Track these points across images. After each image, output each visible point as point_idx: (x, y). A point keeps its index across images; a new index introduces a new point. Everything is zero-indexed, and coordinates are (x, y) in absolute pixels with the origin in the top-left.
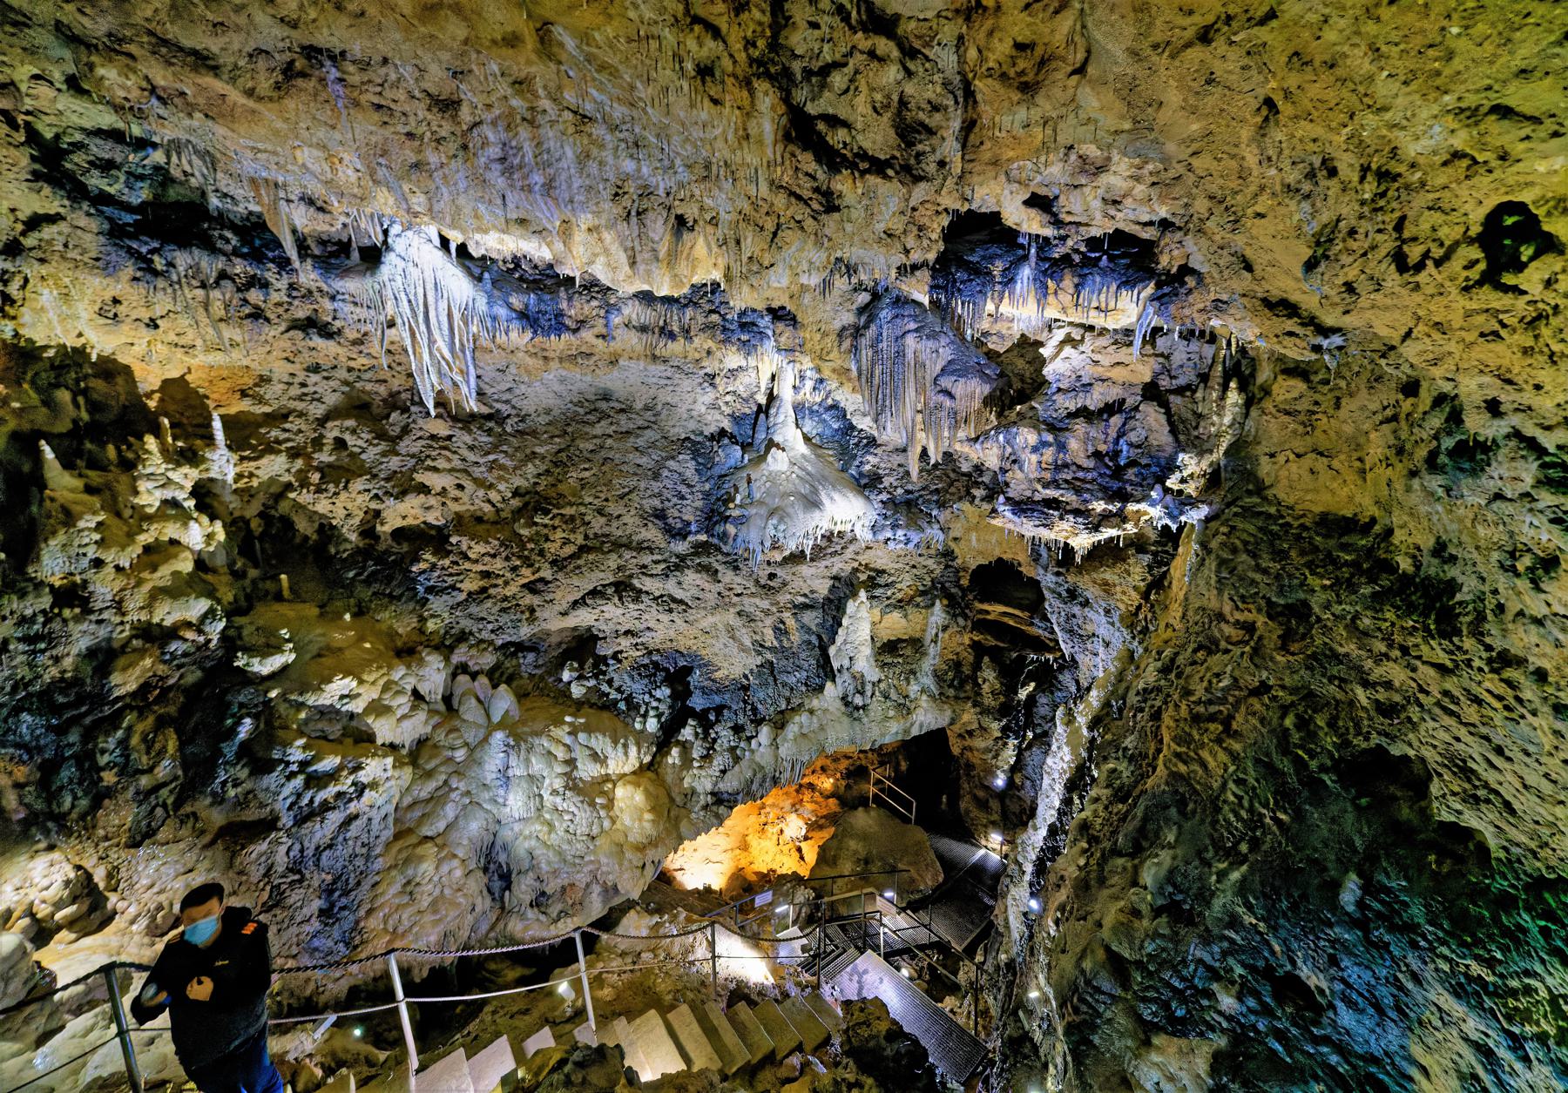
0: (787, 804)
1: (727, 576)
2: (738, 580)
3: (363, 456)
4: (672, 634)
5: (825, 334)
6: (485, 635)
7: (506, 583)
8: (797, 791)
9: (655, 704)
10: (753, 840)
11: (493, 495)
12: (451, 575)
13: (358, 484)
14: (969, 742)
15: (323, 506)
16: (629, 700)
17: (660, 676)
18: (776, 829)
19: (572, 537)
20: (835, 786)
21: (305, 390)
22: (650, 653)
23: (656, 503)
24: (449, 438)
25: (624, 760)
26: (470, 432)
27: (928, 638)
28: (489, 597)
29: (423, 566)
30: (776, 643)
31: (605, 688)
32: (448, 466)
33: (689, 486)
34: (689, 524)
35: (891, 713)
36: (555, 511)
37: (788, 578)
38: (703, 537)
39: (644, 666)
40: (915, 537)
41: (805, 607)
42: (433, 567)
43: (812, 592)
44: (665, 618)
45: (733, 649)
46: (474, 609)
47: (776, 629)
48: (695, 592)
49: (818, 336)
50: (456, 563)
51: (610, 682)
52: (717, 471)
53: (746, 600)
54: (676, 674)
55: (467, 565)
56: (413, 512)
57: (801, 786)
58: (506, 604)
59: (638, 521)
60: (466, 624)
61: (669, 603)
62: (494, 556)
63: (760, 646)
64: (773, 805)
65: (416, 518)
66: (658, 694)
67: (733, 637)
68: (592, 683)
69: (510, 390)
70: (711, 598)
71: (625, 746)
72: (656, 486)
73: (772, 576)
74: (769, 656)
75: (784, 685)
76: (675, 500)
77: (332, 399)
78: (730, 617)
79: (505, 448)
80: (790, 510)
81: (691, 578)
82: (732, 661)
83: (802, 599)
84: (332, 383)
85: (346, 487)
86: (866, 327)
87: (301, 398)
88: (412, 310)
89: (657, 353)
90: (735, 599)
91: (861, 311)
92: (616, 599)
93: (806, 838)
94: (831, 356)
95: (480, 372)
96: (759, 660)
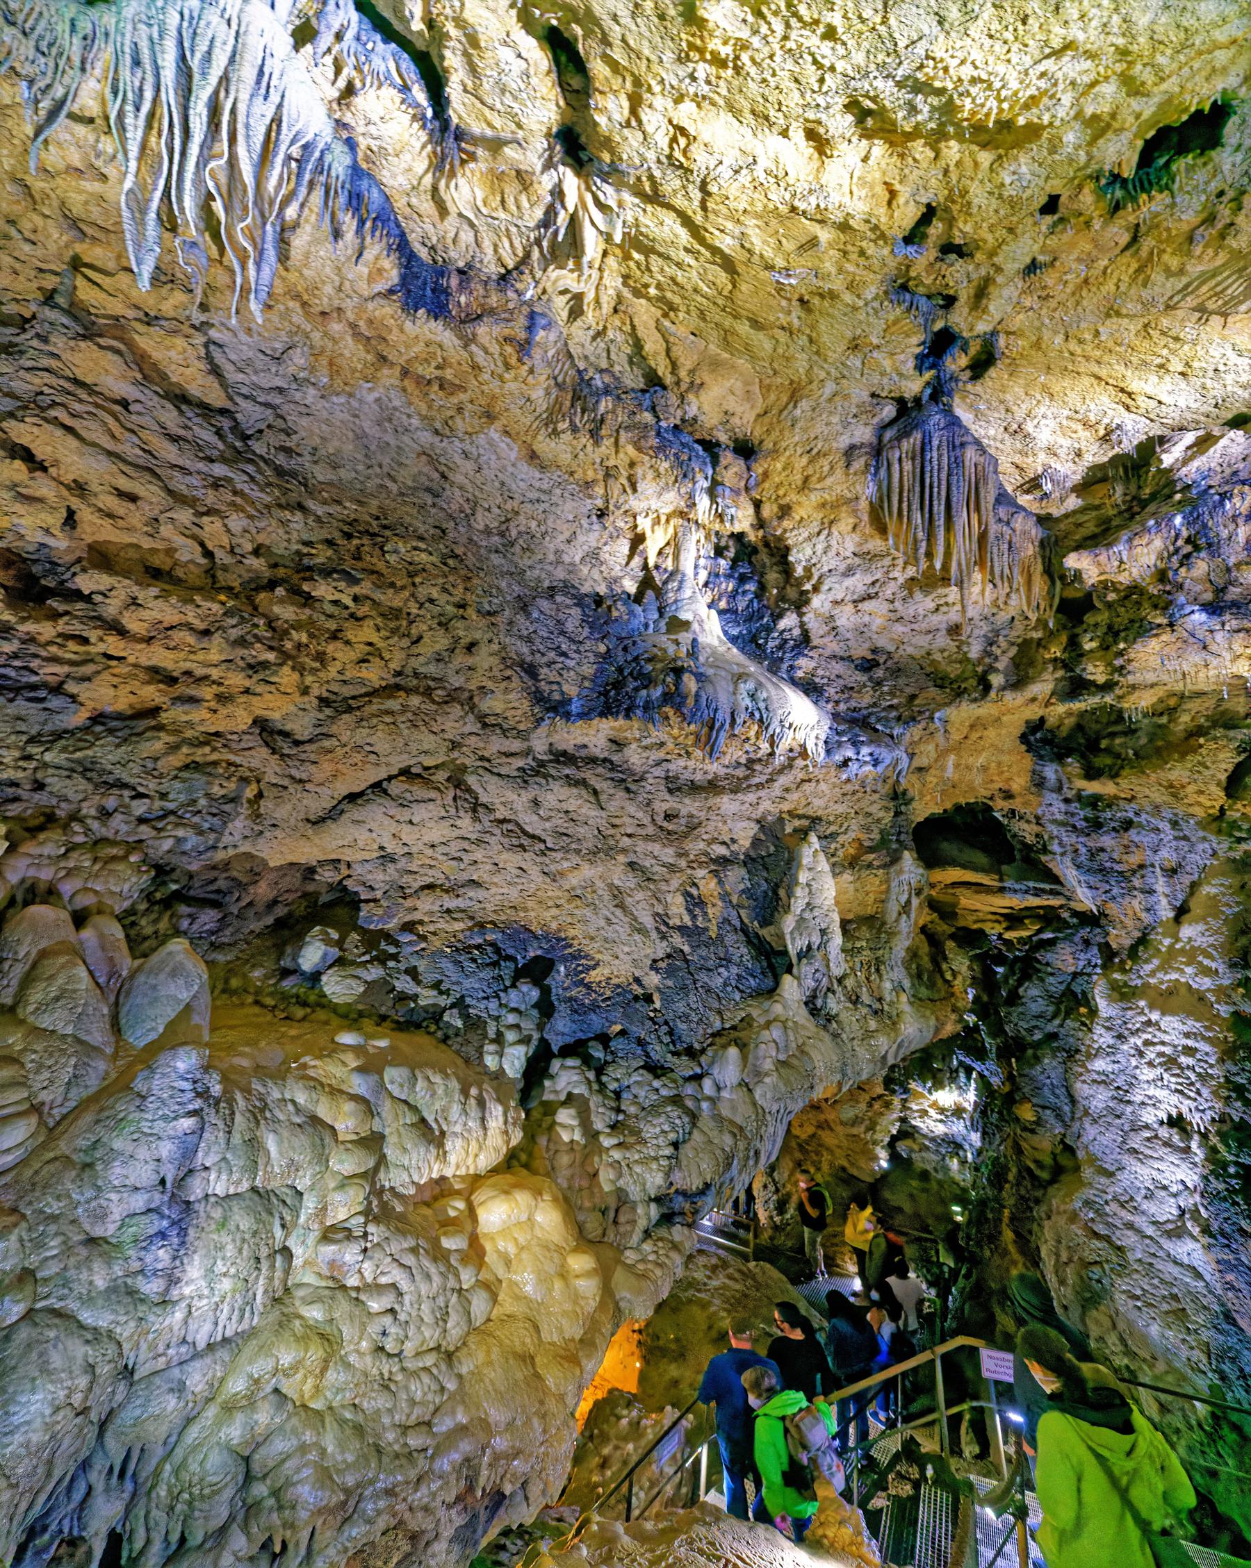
6: (119, 826)
9: (511, 1019)
11: (212, 529)
16: (460, 1004)
17: (507, 970)
22: (481, 926)
25: (478, 1140)
27: (892, 915)
28: (160, 728)
30: (687, 920)
31: (404, 984)
39: (478, 947)
41: (724, 862)
44: (511, 860)
45: (622, 928)
46: (106, 753)
48: (559, 822)
51: (413, 973)
53: (641, 846)
54: (533, 963)
60: (68, 790)
66: (513, 998)
68: (375, 973)
71: (481, 1103)
82: (621, 955)
90: (626, 841)
96: (661, 949)
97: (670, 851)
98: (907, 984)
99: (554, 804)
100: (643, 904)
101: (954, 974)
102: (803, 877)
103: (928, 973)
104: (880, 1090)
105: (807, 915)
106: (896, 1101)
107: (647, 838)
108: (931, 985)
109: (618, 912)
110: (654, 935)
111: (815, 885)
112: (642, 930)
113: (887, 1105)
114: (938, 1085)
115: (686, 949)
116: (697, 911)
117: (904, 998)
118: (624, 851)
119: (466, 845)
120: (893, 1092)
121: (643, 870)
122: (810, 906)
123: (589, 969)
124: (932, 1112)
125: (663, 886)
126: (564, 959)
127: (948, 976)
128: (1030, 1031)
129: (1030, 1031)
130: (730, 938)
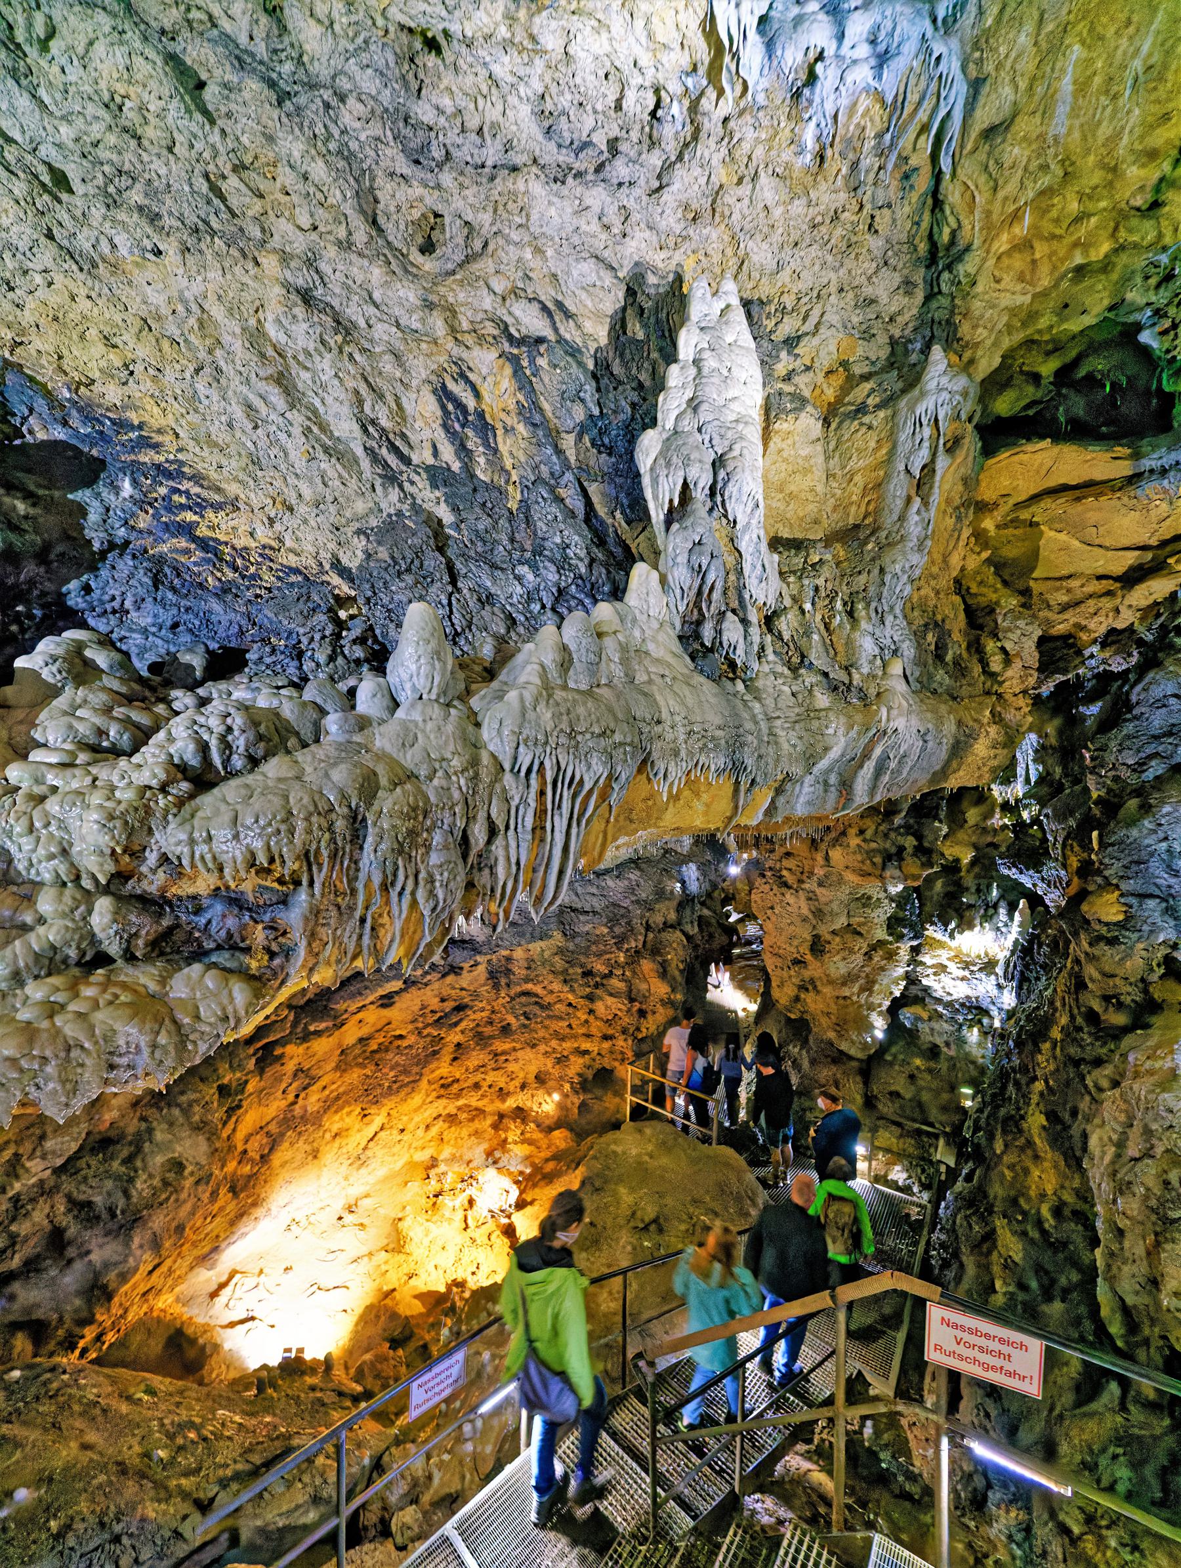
0: (478, 1153)
8: (495, 1127)
10: (416, 1229)
14: (814, 969)
18: (462, 1199)
20: (561, 1106)
30: (448, 454)
35: (822, 700)
57: (501, 1116)
64: (453, 1159)
67: (282, 380)
75: (487, 600)
93: (520, 1205)
97: (408, 293)
98: (908, 650)
100: (336, 391)
101: (1008, 659)
102: (688, 342)
103: (956, 646)
104: (881, 934)
105: (687, 425)
106: (904, 949)
108: (959, 669)
111: (710, 362)
112: (336, 452)
113: (891, 956)
114: (965, 924)
115: (444, 513)
116: (473, 442)
117: (896, 668)
120: (900, 937)
121: (343, 326)
122: (694, 405)
123: (199, 506)
124: (952, 966)
126: (135, 470)
127: (996, 665)
128: (1140, 767)
129: (1140, 767)
130: (545, 513)
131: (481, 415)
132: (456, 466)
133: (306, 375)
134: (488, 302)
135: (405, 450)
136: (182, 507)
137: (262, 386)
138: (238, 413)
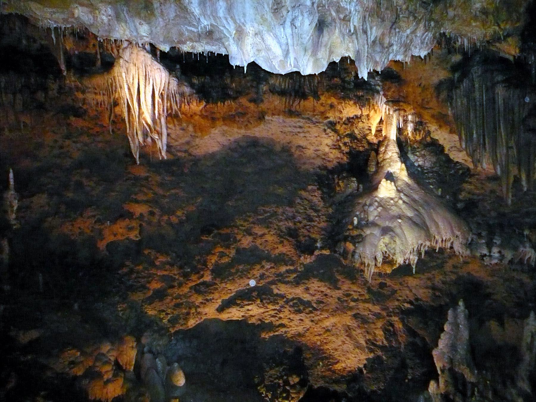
1: (346, 286)
2: (355, 288)
3: (94, 193)
4: (300, 329)
5: (425, 89)
7: (180, 285)
12: (144, 277)
13: (89, 212)
15: (67, 228)
19: (227, 251)
21: (62, 151)
23: (291, 224)
24: (146, 178)
26: (160, 174)
29: (125, 270)
32: (145, 198)
33: (316, 211)
34: (316, 241)
36: (216, 231)
37: (396, 287)
38: (326, 252)
40: (509, 255)
42: (132, 271)
43: (417, 299)
45: (349, 346)
47: (385, 330)
48: (318, 296)
49: (419, 90)
50: (146, 269)
52: (338, 198)
53: (361, 305)
55: (153, 271)
56: (121, 231)
58: (179, 301)
59: (276, 239)
61: (300, 306)
62: (172, 265)
63: (372, 345)
65: (122, 235)
69: (188, 143)
70: (333, 302)
72: (290, 211)
73: (382, 285)
74: (380, 353)
76: (305, 222)
77: (77, 155)
78: (347, 320)
79: (182, 185)
80: (398, 231)
81: (315, 285)
83: (407, 306)
84: (79, 145)
85: (81, 215)
86: (460, 81)
87: (59, 156)
88: (131, 95)
89: (293, 109)
90: (352, 304)
91: (454, 68)
92: (259, 302)
94: (431, 105)
95: (170, 131)
99: (316, 288)
100: (360, 335)
107: (366, 301)
109: (348, 338)
110: (367, 350)
118: (351, 309)
119: (276, 312)
125: (373, 326)
131: (394, 331)
132: (387, 345)
133: (354, 332)
134: (397, 303)
135: (375, 342)
136: (330, 365)
137: (346, 337)
138: (340, 343)
